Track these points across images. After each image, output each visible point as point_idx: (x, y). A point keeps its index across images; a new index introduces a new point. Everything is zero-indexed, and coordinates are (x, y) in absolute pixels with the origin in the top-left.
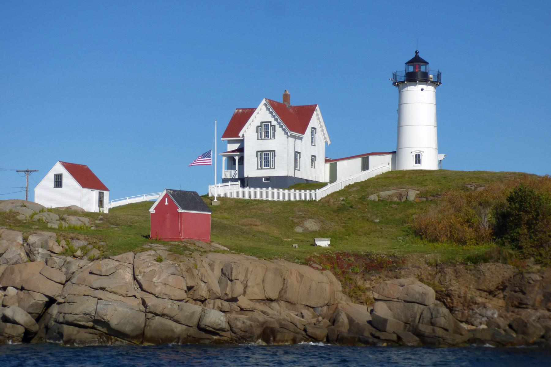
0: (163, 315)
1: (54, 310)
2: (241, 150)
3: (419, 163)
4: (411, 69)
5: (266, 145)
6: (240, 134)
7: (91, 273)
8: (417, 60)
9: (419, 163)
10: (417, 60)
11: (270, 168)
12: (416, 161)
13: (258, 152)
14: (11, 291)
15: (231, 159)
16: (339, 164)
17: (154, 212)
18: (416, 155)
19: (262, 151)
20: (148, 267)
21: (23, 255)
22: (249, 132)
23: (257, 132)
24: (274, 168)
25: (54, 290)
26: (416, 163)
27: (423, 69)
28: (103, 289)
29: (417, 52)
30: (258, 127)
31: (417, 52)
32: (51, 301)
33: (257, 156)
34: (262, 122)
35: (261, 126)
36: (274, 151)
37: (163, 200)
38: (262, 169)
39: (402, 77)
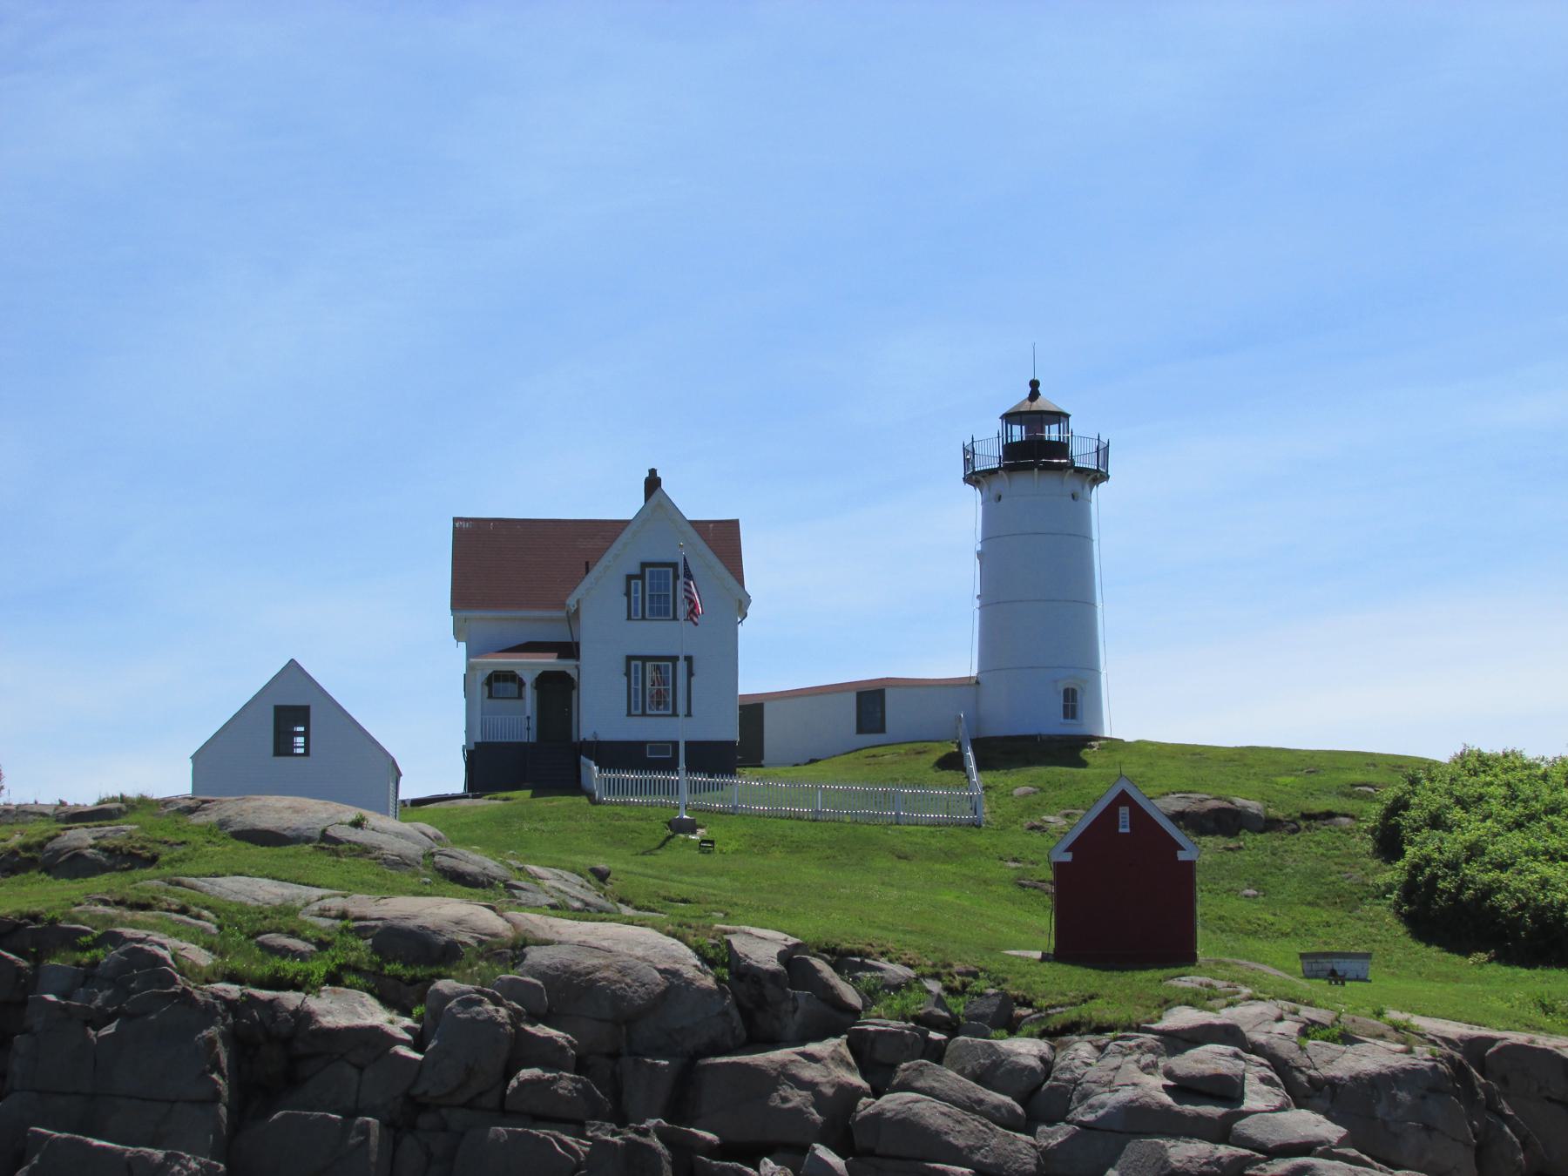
2: (569, 650)
3: (1074, 716)
4: (1018, 433)
5: (656, 637)
6: (571, 602)
9: (1074, 716)
11: (675, 714)
12: (1065, 707)
13: (629, 659)
17: (1068, 857)
18: (1066, 691)
19: (645, 659)
20: (1330, 1062)
21: (735, 1013)
23: (628, 594)
24: (689, 714)
26: (1066, 716)
28: (1306, 1148)
29: (1034, 384)
30: (630, 578)
31: (1034, 384)
33: (628, 674)
34: (644, 565)
35: (641, 577)
36: (689, 659)
37: (1110, 813)
38: (644, 714)
39: (990, 456)
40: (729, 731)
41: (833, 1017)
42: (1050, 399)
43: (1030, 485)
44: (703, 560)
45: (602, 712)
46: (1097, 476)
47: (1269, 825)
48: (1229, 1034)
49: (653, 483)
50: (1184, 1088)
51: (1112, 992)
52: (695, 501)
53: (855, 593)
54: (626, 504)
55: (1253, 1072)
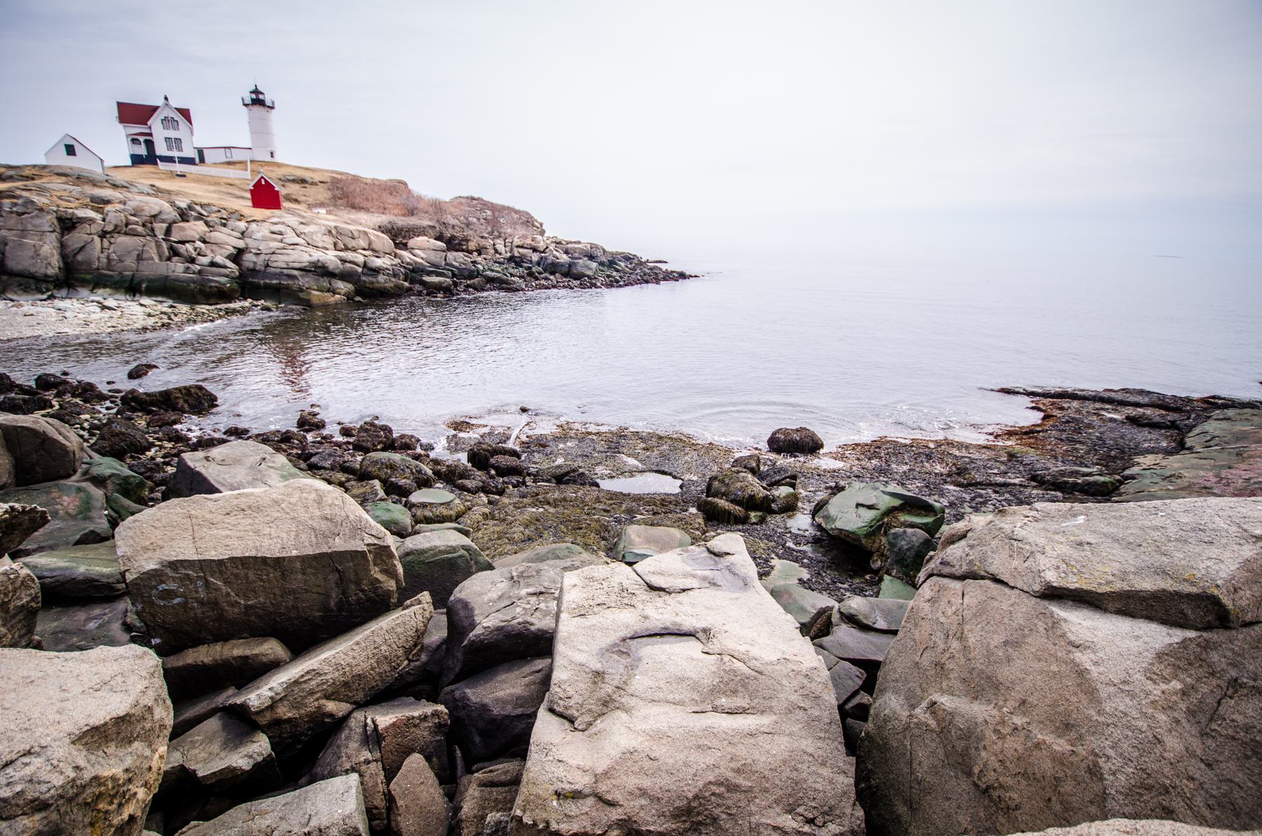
0: (350, 262)
1: (249, 259)
2: (151, 135)
4: (254, 96)
5: (172, 134)
7: (273, 233)
8: (256, 92)
10: (256, 92)
14: (199, 244)
15: (135, 141)
16: (205, 151)
22: (155, 123)
25: (241, 244)
27: (261, 97)
32: (240, 252)
39: (248, 101)
40: (193, 154)
41: (200, 217)
42: (260, 89)
43: (256, 109)
44: (178, 117)
45: (161, 149)
46: (272, 108)
47: (313, 184)
48: (283, 223)
49: (166, 98)
50: (273, 233)
51: (260, 213)
52: (174, 103)
53: (219, 127)
54: (159, 102)
55: (289, 230)
